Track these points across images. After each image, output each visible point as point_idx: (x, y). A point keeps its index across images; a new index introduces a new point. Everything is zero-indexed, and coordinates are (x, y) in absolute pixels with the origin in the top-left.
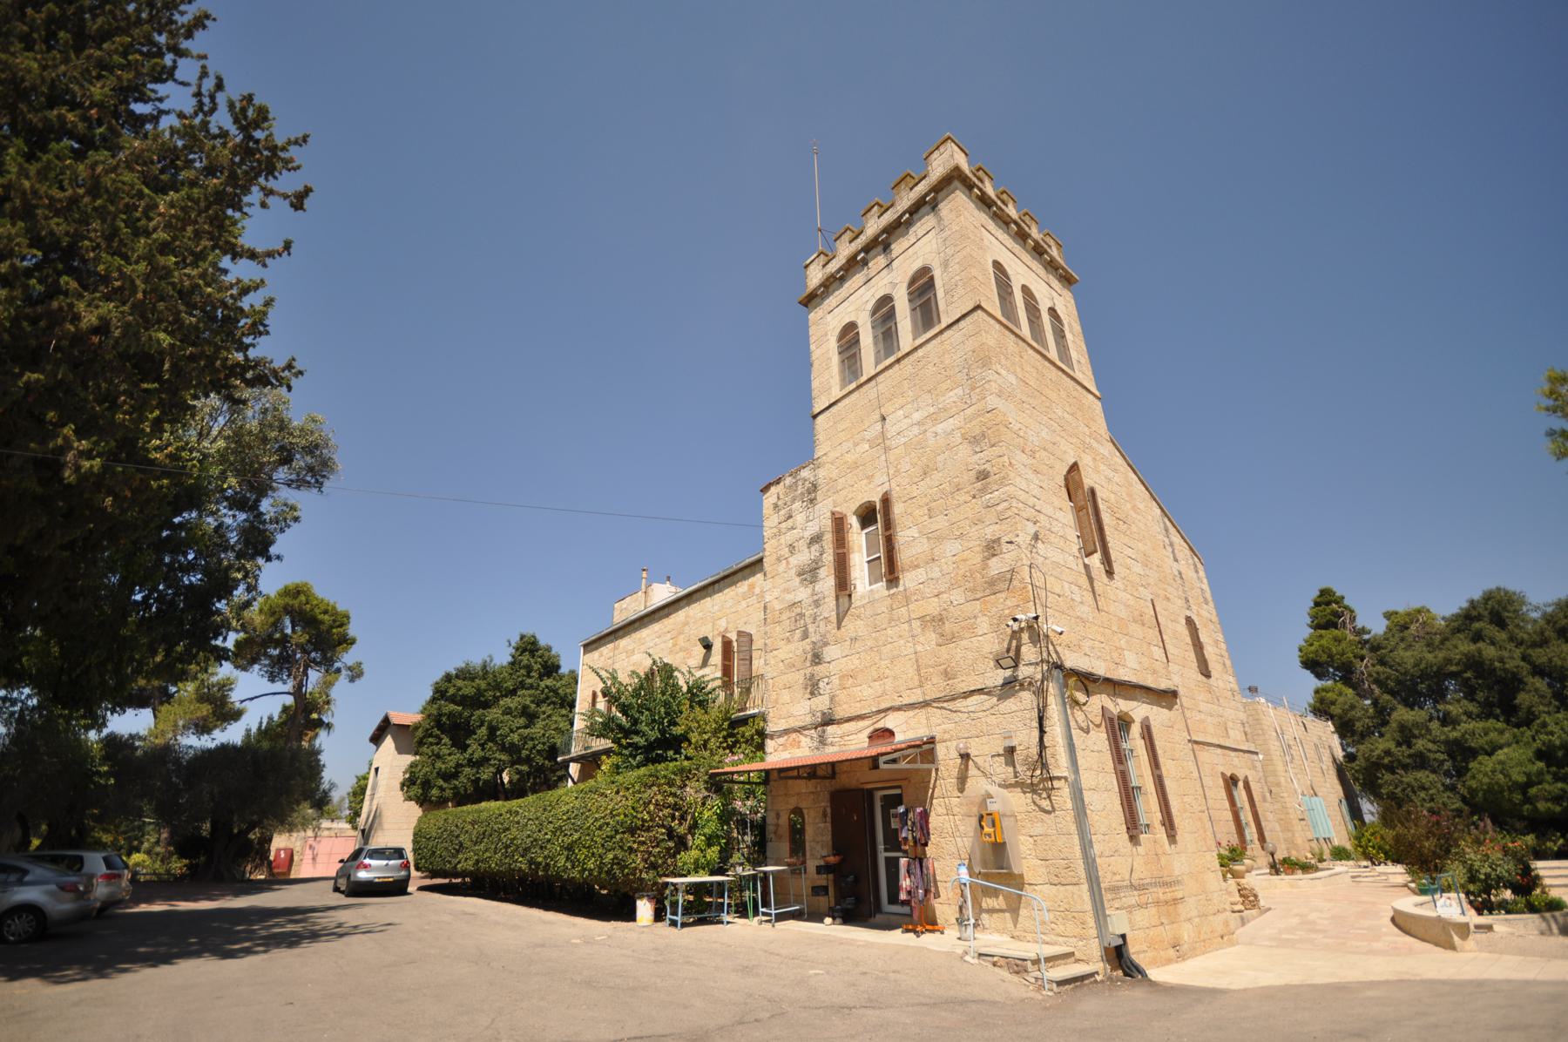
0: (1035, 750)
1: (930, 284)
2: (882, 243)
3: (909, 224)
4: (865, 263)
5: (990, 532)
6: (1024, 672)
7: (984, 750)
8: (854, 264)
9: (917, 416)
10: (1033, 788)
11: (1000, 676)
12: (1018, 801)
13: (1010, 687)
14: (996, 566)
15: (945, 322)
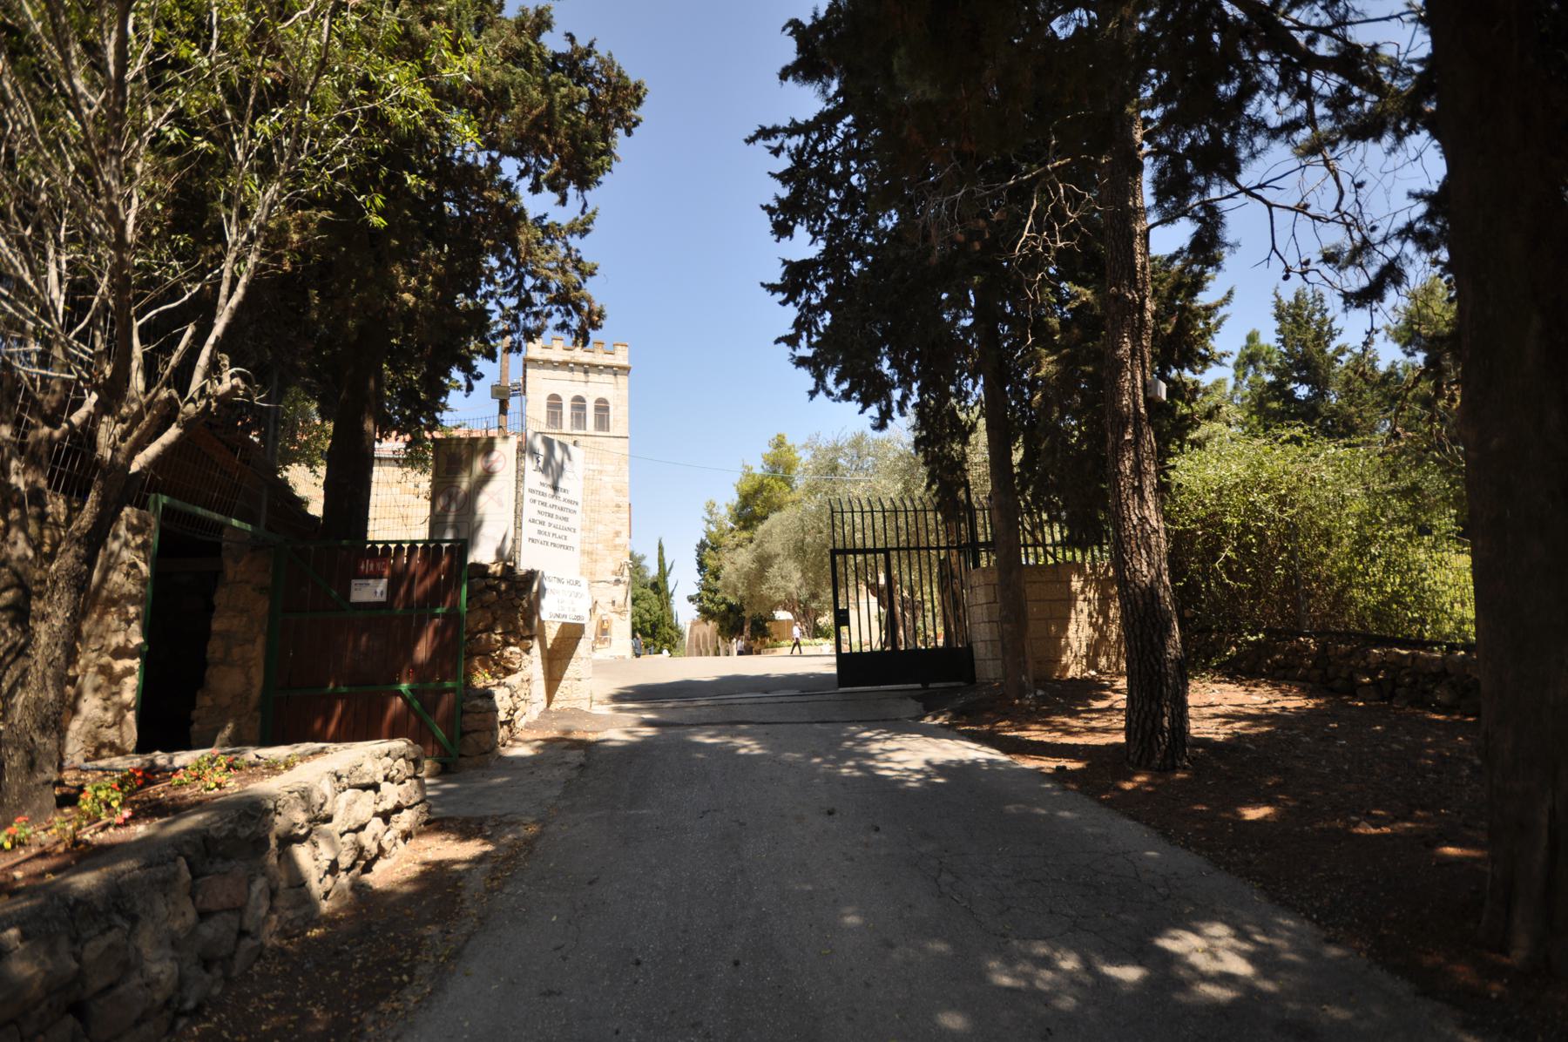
0: (622, 602)
1: (607, 409)
2: (587, 368)
3: (600, 372)
4: (572, 370)
5: (618, 528)
6: (622, 579)
7: (604, 601)
8: (564, 365)
9: (592, 467)
10: (620, 613)
11: (614, 578)
12: (615, 617)
13: (618, 582)
14: (618, 541)
15: (611, 433)
